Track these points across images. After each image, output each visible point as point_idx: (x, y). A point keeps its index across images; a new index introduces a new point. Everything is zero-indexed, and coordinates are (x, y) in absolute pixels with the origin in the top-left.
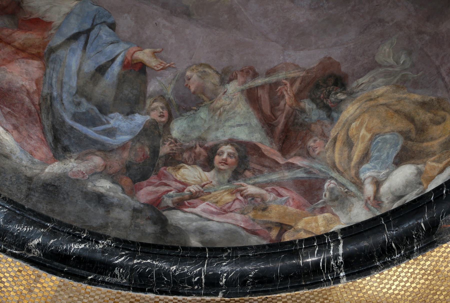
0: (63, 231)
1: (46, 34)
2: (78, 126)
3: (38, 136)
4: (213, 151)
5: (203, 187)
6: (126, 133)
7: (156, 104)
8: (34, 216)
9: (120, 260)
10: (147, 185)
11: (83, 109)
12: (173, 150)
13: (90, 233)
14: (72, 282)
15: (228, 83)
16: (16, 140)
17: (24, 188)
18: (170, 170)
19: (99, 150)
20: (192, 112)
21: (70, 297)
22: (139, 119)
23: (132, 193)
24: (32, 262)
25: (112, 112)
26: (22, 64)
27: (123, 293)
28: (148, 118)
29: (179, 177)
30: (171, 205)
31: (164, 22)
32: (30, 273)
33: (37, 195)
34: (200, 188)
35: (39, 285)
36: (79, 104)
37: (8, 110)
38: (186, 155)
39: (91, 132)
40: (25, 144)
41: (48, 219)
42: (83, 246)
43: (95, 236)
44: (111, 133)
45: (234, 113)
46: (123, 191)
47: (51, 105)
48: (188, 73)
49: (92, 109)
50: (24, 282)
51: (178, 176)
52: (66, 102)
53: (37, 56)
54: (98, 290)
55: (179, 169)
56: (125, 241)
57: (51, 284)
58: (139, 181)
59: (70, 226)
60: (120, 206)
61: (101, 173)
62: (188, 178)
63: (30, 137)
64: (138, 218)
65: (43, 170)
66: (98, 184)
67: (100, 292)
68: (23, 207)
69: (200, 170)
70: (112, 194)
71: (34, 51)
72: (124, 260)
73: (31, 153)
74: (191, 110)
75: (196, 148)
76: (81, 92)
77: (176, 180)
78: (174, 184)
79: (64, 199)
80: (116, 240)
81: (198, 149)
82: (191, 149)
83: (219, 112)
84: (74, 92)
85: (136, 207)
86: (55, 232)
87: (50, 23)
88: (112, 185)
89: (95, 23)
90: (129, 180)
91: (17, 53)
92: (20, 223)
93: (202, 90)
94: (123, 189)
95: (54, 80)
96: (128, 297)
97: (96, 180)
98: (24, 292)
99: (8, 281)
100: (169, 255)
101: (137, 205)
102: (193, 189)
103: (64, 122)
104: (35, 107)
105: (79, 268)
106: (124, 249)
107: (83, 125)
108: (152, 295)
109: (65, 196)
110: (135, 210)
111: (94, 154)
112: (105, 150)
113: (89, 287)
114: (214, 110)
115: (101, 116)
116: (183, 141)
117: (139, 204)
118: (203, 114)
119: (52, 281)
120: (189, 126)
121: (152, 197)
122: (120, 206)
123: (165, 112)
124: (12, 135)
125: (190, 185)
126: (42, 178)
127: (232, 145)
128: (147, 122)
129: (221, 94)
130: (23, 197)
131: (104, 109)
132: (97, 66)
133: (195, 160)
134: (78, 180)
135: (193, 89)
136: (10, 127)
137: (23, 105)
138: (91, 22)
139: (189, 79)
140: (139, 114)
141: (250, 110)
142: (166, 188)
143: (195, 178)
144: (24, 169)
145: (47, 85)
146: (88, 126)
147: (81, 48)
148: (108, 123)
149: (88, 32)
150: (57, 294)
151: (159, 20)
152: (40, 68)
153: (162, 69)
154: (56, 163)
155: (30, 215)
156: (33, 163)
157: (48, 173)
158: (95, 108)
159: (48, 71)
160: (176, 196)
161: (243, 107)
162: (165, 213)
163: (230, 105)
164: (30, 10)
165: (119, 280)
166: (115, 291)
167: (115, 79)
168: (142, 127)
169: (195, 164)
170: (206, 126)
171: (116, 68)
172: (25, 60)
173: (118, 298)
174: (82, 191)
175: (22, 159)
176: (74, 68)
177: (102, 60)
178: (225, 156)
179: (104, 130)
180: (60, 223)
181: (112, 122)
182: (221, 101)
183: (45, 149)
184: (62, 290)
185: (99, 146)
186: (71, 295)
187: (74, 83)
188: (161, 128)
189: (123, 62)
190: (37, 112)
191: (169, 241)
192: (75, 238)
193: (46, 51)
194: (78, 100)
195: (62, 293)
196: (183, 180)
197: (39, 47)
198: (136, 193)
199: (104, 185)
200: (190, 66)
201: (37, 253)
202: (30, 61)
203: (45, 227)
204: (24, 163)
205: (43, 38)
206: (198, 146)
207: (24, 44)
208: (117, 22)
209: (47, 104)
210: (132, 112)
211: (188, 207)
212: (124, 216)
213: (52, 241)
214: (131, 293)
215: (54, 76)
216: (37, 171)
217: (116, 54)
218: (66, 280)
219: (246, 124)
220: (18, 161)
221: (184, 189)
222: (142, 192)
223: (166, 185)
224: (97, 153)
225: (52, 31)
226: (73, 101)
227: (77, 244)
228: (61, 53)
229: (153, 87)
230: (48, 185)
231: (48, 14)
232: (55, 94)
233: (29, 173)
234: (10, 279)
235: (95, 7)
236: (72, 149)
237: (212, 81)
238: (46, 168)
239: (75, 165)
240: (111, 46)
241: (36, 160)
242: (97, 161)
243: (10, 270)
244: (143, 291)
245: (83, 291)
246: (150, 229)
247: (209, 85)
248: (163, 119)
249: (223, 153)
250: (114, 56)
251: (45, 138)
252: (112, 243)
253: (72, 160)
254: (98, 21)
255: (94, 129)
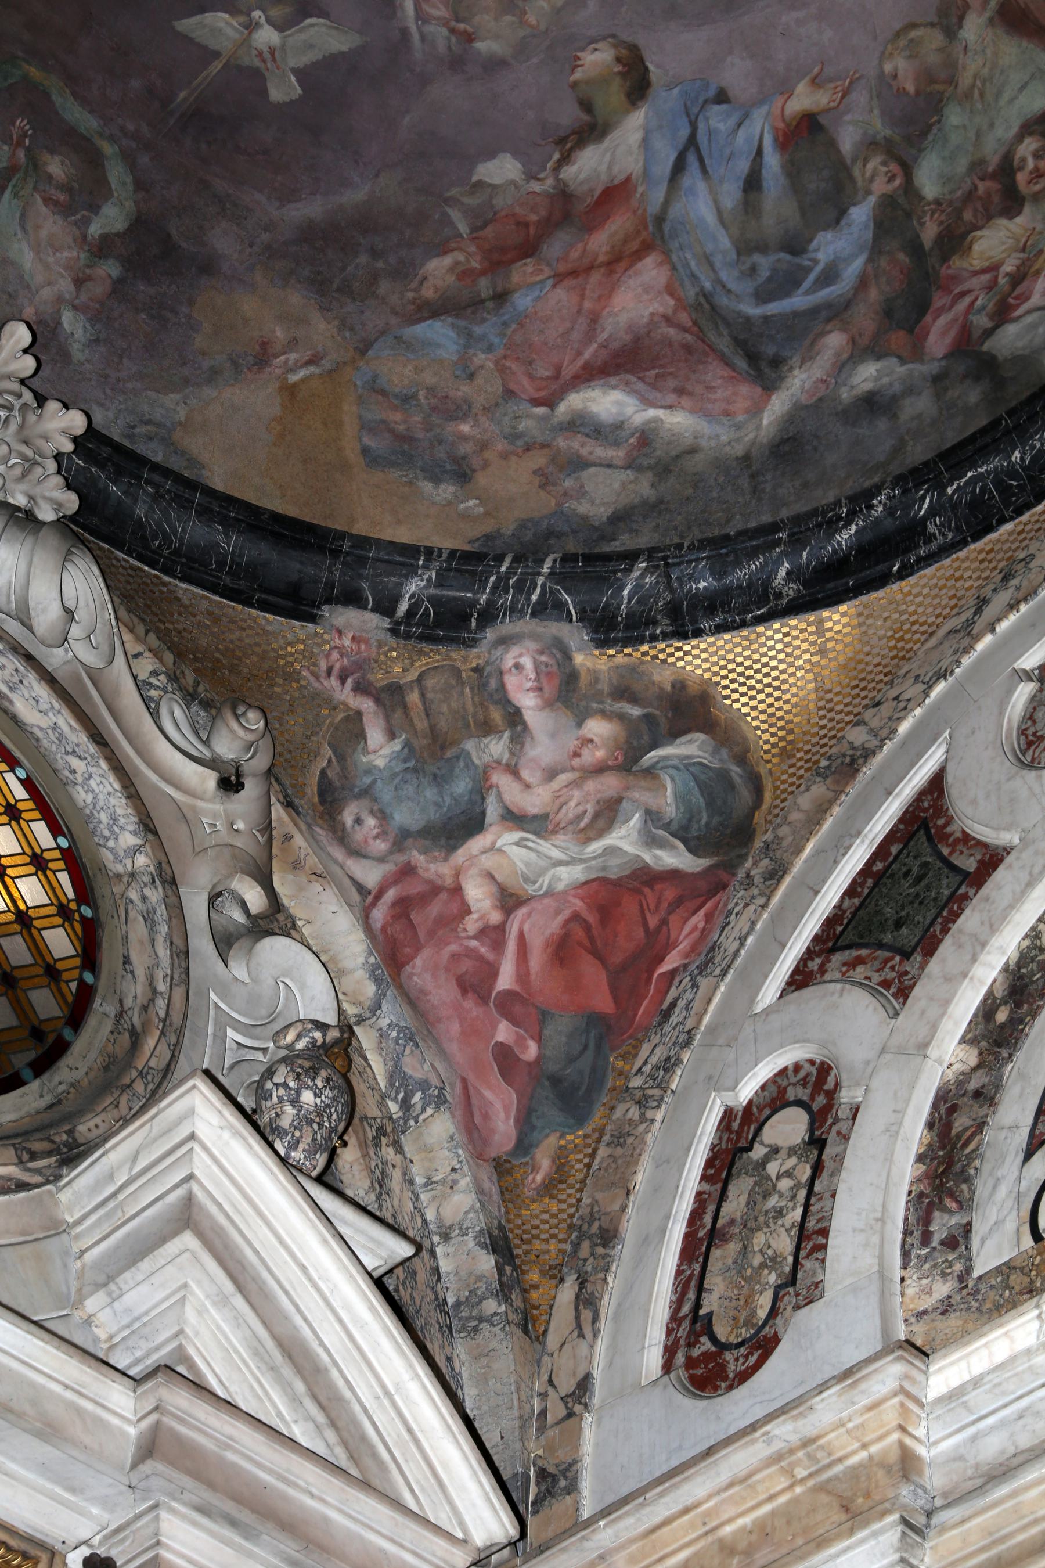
0: (809, 529)
1: (634, 203)
2: (774, 308)
3: (722, 377)
4: (1007, 168)
5: (1023, 250)
6: (854, 256)
7: (870, 166)
8: (751, 539)
9: (926, 506)
10: (934, 320)
11: (764, 274)
12: (942, 222)
13: (851, 499)
14: (874, 595)
15: (960, 27)
16: (692, 411)
17: (745, 482)
18: (957, 263)
19: (829, 320)
20: (935, 130)
21: (885, 619)
22: (860, 214)
23: (917, 353)
24: (797, 607)
25: (811, 240)
26: (631, 282)
27: (962, 554)
28: (872, 200)
29: (977, 264)
30: (989, 325)
31: (795, 14)
32: (803, 625)
33: (769, 477)
34: (1022, 255)
35: (828, 635)
36: (753, 270)
37: (653, 372)
38: (968, 215)
39: (798, 301)
40: (710, 406)
41: (775, 527)
42: (854, 528)
43: (861, 501)
44: (829, 276)
45: (1002, 72)
46: (902, 360)
47: (713, 308)
48: (888, 67)
49: (779, 260)
50: (805, 646)
51: (975, 262)
52: (732, 285)
53: (646, 248)
54: (921, 578)
55: (970, 248)
56: (914, 471)
57: (845, 620)
58: (918, 321)
59: (815, 512)
60: (910, 390)
61: (851, 357)
62: (992, 254)
63: (710, 388)
64: (946, 389)
65: (759, 427)
66: (856, 380)
67: (926, 580)
68: (726, 537)
69: (1003, 222)
70: (886, 380)
71: (635, 245)
72: (931, 501)
73: (727, 414)
74: (930, 127)
75: (976, 188)
76: (745, 248)
77: (976, 273)
78: (976, 282)
79: (815, 449)
80: (899, 480)
81: (982, 187)
82: (970, 195)
83: (976, 91)
84: (735, 256)
85: (934, 372)
86: (797, 540)
87: (628, 179)
88: (879, 365)
89: (693, 118)
90: (902, 333)
91: (611, 272)
92: (738, 564)
93: (927, 77)
94: (899, 357)
95: (693, 264)
96: (972, 556)
97: (850, 376)
98: (815, 659)
99: (781, 661)
100: (995, 441)
101: (934, 368)
102: (1008, 268)
103: (748, 319)
104: (691, 333)
105: (869, 567)
106: (918, 486)
107: (781, 298)
108: (1009, 526)
109: (815, 443)
110: (938, 380)
111: (823, 334)
112: (835, 313)
113: (903, 583)
114: (968, 95)
115: (797, 260)
116: (950, 193)
117: (936, 364)
118: (954, 117)
119: (843, 615)
120: (944, 158)
121: (953, 333)
122: (910, 390)
123: (894, 167)
124: (683, 408)
125: (1002, 264)
126: (765, 440)
127: (1030, 134)
128: (874, 209)
129: (961, 56)
130: (748, 497)
131: (795, 245)
132: (741, 183)
133: (987, 210)
134: (821, 400)
135: (911, 88)
136: (671, 398)
137: (670, 345)
138: (685, 119)
139: (895, 77)
140: (854, 205)
141: (1025, 43)
142: (967, 300)
143: (1004, 243)
144: (728, 449)
145: (687, 283)
146: (788, 294)
147: (700, 176)
148: (816, 262)
149: (692, 141)
150: (864, 628)
151: (784, 19)
152: (661, 264)
153: (843, 97)
154: (774, 397)
155: (743, 542)
156: (738, 427)
157: (770, 424)
158: (782, 255)
159: (674, 258)
160: (989, 300)
161: (1012, 51)
162: (985, 348)
163: (988, 65)
164: (585, 187)
165: (940, 540)
166: (947, 562)
167: (782, 180)
168: (872, 225)
169: (989, 218)
170: (972, 134)
171: (772, 160)
172: (631, 272)
173: (958, 568)
174: (837, 414)
175: (718, 436)
176: (710, 217)
177: (743, 166)
178: (1031, 163)
179: (817, 280)
180: (797, 520)
181: (821, 256)
182: (971, 68)
183: (745, 389)
184: (867, 617)
185: (824, 314)
186: (886, 615)
187: (725, 242)
188: (901, 200)
189: (776, 140)
190: (698, 338)
191: (1017, 393)
192: (833, 525)
193: (651, 228)
194: (748, 265)
195: (870, 621)
196: (987, 264)
197: (638, 232)
198: (923, 347)
199: (867, 375)
200: (883, 53)
201: (791, 590)
202: (639, 265)
203: (778, 542)
204: (724, 438)
205: (635, 212)
206: (977, 182)
207: (613, 247)
208: (723, 84)
209: (706, 310)
210: (843, 212)
211: (1018, 306)
212: (920, 406)
213: (805, 554)
214: (972, 546)
215: (689, 256)
216: (751, 436)
217: (757, 138)
218: (864, 598)
219: (1033, 76)
220: (713, 443)
221: (996, 277)
222: (932, 338)
223: (963, 294)
224: (828, 328)
225: (640, 189)
226: (742, 272)
227: (844, 531)
228: (676, 211)
229: (848, 140)
230: (778, 446)
231: (616, 169)
232: (708, 285)
233: (739, 450)
234: (782, 656)
235: (676, 91)
236: (786, 353)
237: (934, 47)
238: (761, 419)
239: (804, 376)
240: (741, 134)
241: (740, 418)
242: (835, 341)
243: (771, 643)
244: (989, 529)
245: (899, 597)
246: (973, 395)
247: (933, 59)
248: (898, 182)
249: (1024, 160)
250: (756, 144)
251: (734, 370)
252: (893, 490)
253: (796, 372)
254: (695, 110)
255: (800, 291)
